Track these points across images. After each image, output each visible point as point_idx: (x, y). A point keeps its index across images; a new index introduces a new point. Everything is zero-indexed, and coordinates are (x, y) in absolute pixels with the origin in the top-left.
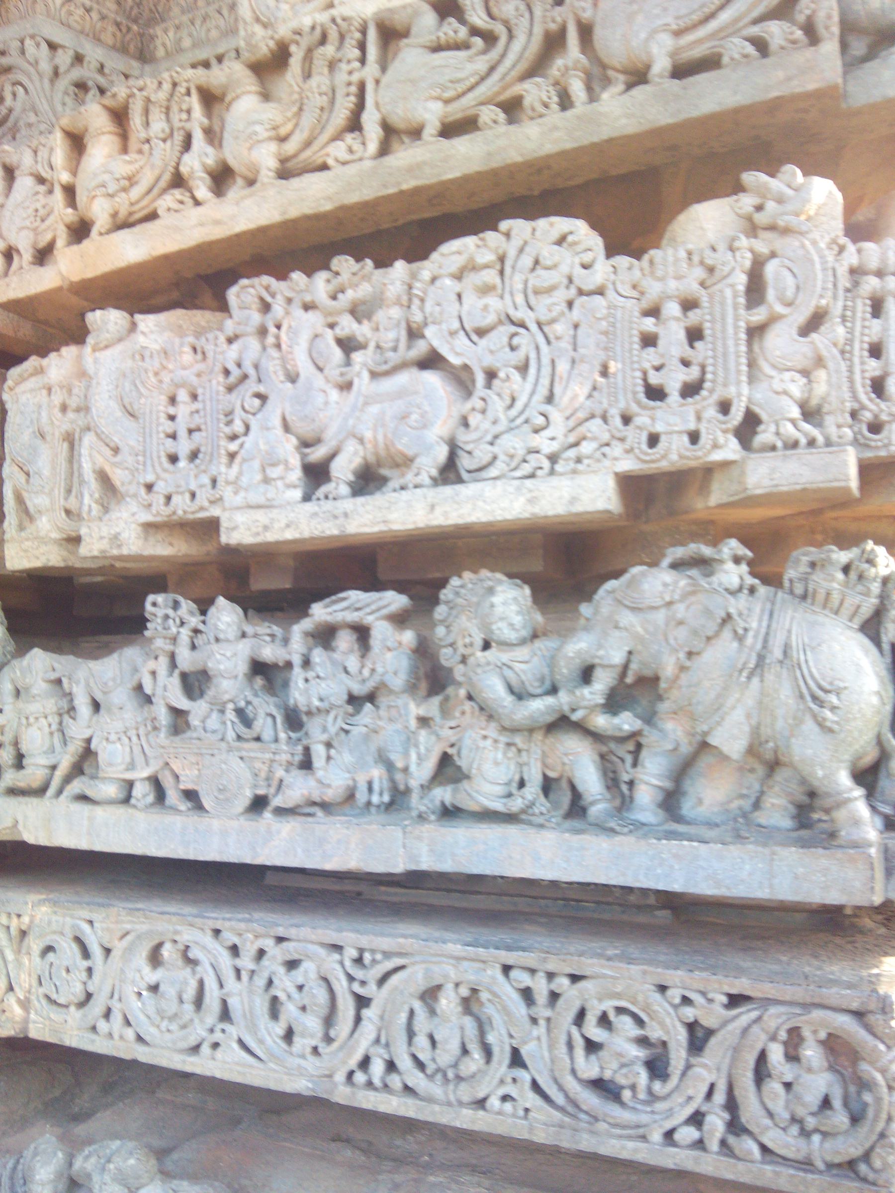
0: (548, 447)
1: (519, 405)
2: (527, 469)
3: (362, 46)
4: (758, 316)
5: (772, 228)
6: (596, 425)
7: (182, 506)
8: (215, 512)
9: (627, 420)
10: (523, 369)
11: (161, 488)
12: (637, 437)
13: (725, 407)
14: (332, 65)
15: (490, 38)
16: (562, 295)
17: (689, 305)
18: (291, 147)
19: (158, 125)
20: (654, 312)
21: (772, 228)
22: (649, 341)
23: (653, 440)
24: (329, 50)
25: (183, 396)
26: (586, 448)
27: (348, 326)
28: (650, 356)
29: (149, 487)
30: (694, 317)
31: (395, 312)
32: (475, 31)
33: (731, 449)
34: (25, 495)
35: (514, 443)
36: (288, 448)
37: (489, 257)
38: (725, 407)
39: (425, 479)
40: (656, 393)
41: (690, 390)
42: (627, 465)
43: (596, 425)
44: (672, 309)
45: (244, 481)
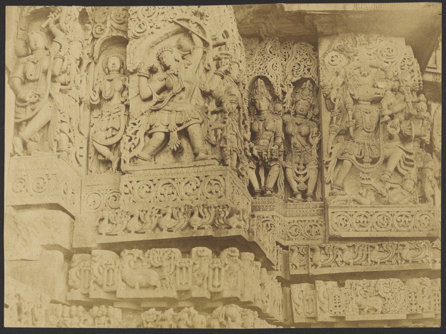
0: (397, 310)
1: (393, 303)
2: (395, 313)
3: (368, 248)
4: (423, 296)
5: (424, 284)
6: (403, 308)
7: (338, 314)
8: (344, 315)
9: (408, 307)
10: (393, 299)
11: (334, 311)
12: (409, 310)
13: (420, 307)
14: (363, 250)
15: (387, 251)
16: (398, 289)
17: (415, 293)
18: (355, 260)
19: (331, 253)
20: (410, 293)
21: (424, 284)
22: (410, 297)
23: (411, 310)
24: (362, 248)
25: (337, 297)
26: (403, 310)
27: (365, 289)
28: (410, 299)
29: (331, 311)
30: (416, 295)
31: (373, 288)
32: (384, 250)
33: (421, 312)
34: (298, 309)
35: (393, 309)
36: (356, 307)
37: (388, 283)
38: (420, 307)
39: (379, 313)
40: (411, 304)
41: (416, 304)
42: (408, 313)
43: (403, 308)
44: (413, 293)
45: (349, 311)
